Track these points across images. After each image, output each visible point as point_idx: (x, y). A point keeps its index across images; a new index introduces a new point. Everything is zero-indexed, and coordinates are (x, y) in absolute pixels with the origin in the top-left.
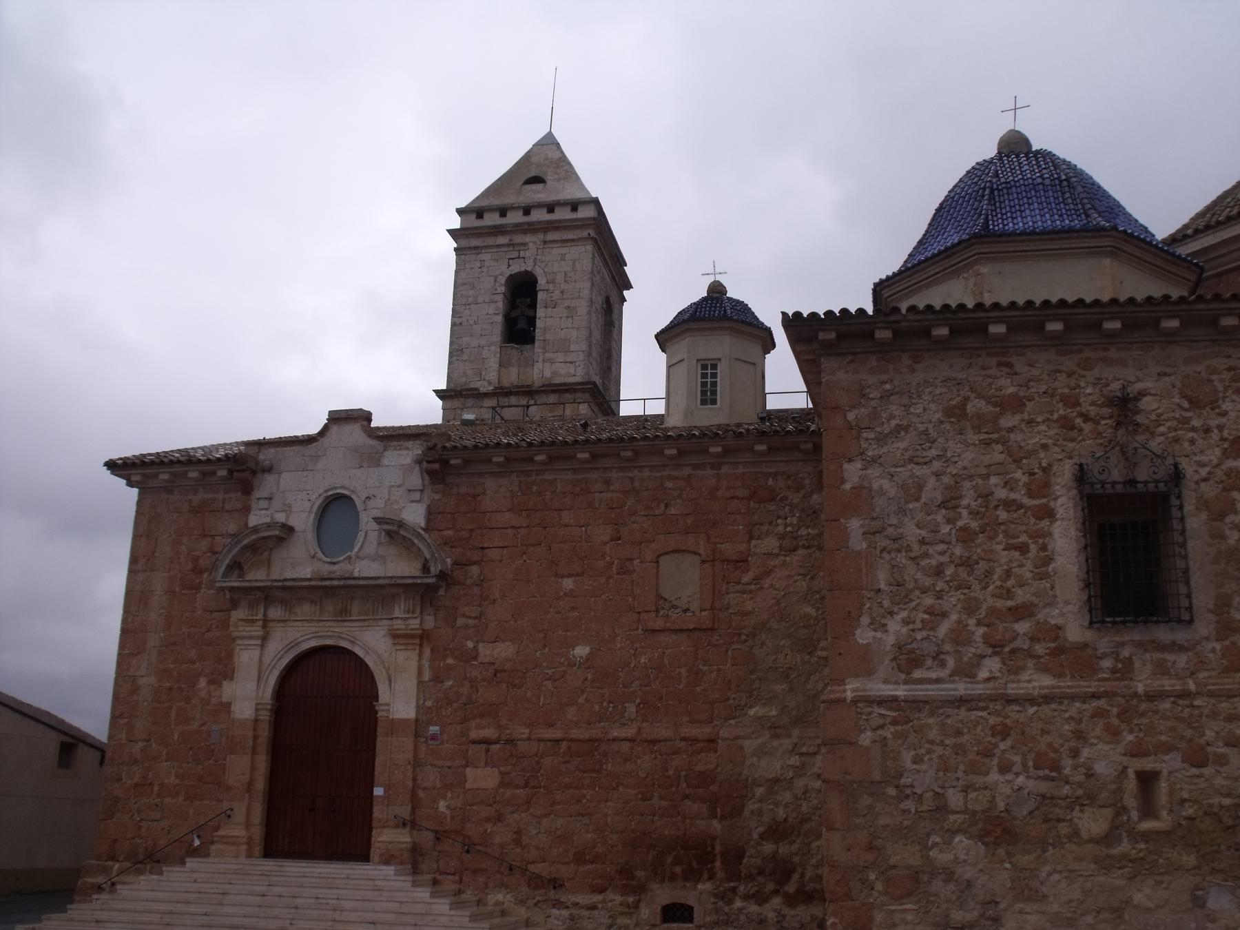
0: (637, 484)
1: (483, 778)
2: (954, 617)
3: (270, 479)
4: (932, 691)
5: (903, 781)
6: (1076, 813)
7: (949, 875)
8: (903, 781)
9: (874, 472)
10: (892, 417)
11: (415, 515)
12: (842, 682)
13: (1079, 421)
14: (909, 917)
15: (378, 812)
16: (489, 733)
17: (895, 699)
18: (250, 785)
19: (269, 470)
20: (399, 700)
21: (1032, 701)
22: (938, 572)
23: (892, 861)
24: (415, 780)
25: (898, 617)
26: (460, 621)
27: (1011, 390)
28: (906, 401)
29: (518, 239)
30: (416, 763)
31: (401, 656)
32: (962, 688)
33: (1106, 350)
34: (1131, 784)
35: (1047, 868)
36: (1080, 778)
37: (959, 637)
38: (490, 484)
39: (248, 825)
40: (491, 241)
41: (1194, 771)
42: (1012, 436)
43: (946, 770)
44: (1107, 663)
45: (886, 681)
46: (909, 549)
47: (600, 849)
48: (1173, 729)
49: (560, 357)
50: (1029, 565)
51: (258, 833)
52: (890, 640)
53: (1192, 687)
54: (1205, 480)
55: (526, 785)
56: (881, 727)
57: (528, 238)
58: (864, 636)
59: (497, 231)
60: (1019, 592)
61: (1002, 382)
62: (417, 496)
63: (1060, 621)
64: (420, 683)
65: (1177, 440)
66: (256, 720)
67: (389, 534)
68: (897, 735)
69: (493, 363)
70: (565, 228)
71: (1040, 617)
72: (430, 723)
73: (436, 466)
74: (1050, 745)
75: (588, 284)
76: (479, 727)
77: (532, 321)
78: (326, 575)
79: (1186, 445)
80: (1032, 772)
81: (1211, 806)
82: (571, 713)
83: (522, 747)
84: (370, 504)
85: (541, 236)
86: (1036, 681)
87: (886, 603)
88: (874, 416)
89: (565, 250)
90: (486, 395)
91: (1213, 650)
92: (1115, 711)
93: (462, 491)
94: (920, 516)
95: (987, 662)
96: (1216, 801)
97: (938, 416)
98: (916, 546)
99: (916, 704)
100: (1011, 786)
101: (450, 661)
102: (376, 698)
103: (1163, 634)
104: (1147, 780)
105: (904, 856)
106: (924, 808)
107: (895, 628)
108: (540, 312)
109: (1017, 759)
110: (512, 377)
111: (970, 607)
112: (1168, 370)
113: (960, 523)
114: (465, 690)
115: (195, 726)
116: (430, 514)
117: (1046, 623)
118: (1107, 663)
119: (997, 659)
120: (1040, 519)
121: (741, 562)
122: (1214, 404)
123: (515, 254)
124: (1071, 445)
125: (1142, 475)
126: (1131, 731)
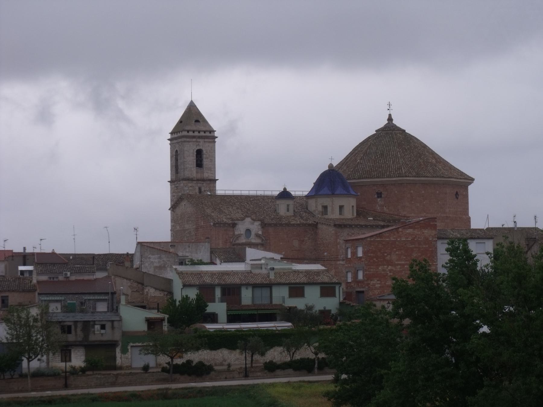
11: (260, 233)
29: (198, 140)
40: (191, 140)
49: (209, 172)
57: (200, 140)
59: (194, 137)
69: (195, 172)
85: (203, 140)
110: (199, 176)
116: (262, 233)
121: (303, 241)
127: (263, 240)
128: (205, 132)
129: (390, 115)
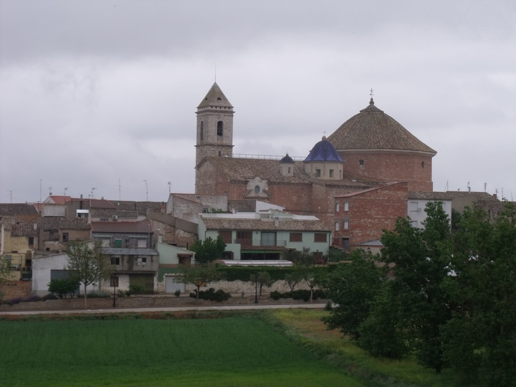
11: (267, 189)
29: (220, 114)
40: (214, 113)
57: (221, 114)
59: (216, 111)
110: (219, 142)
121: (300, 197)
127: (268, 195)
128: (225, 108)
129: (372, 99)
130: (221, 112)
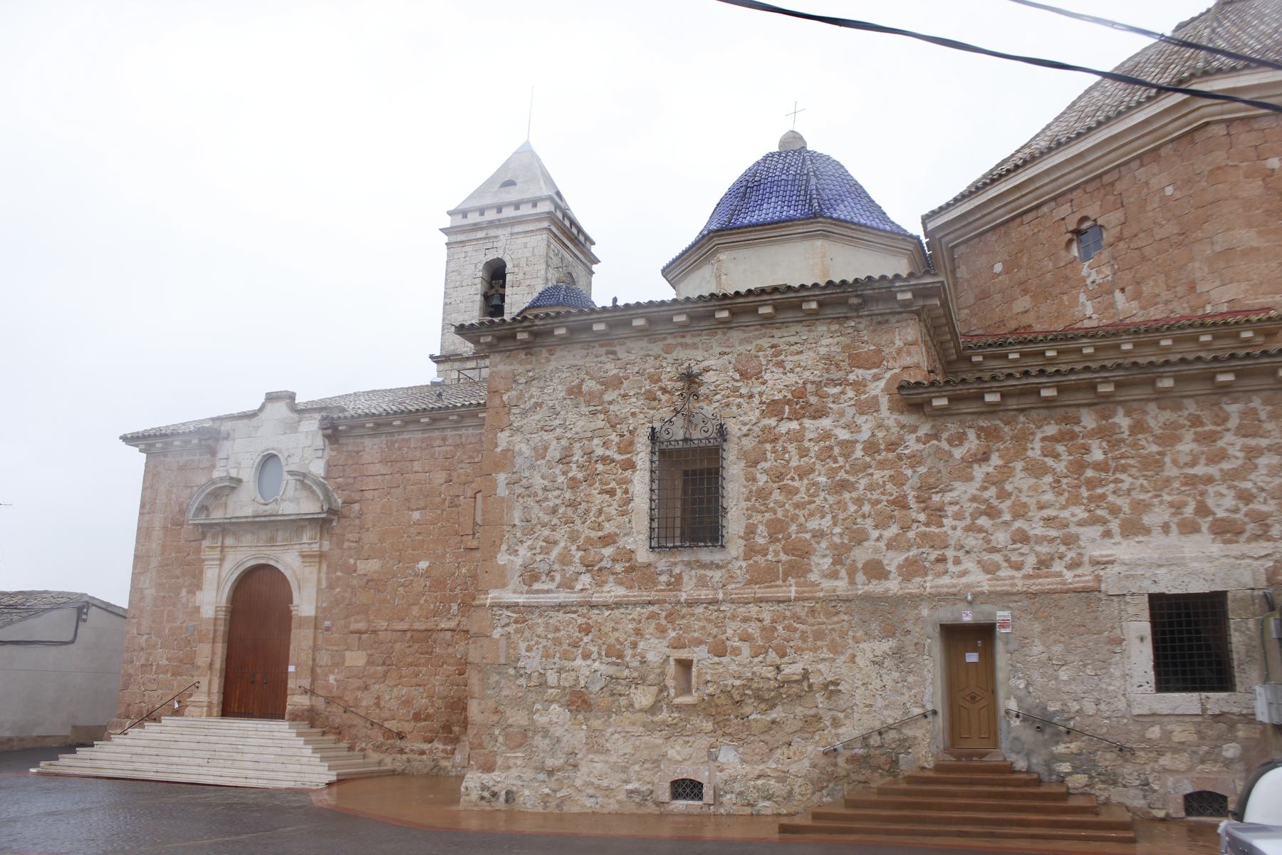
0: (463, 440)
1: (356, 659)
2: (562, 544)
3: (227, 444)
4: (542, 599)
5: (520, 664)
6: (632, 690)
7: (546, 733)
8: (520, 664)
9: (517, 438)
10: (532, 396)
11: (317, 468)
12: (487, 593)
13: (659, 393)
14: (519, 762)
15: (291, 684)
16: (362, 626)
17: (517, 605)
18: (211, 664)
19: (227, 437)
20: (305, 604)
21: (607, 606)
22: (554, 511)
23: (510, 722)
24: (314, 660)
25: (525, 545)
26: (346, 545)
27: (615, 371)
28: (542, 384)
29: (492, 233)
30: (315, 648)
31: (307, 570)
32: (562, 597)
33: (683, 337)
34: (672, 668)
35: (611, 730)
36: (636, 664)
37: (565, 560)
38: (368, 442)
39: (209, 693)
40: (472, 236)
41: (716, 659)
42: (612, 407)
43: (547, 657)
44: (664, 578)
45: (515, 592)
46: (536, 495)
47: (431, 711)
48: (704, 628)
50: (615, 505)
51: (216, 698)
52: (519, 561)
53: (720, 596)
54: (746, 435)
55: (384, 663)
56: (507, 625)
57: (500, 232)
58: (502, 558)
59: (476, 227)
60: (607, 525)
61: (610, 366)
62: (320, 453)
63: (633, 547)
64: (319, 591)
65: (728, 405)
66: (216, 619)
67: (302, 482)
68: (517, 631)
70: (526, 222)
71: (621, 544)
72: (325, 619)
73: (329, 432)
74: (617, 640)
75: (544, 266)
76: (356, 621)
77: (502, 297)
78: (261, 512)
79: (735, 408)
80: (605, 659)
81: (726, 686)
82: (415, 611)
83: (382, 635)
84: (290, 460)
85: (509, 230)
86: (613, 591)
87: (519, 535)
88: (520, 397)
89: (527, 240)
90: (468, 359)
91: (740, 568)
92: (664, 614)
93: (350, 448)
94: (544, 470)
95: (582, 577)
96: (730, 682)
97: (563, 394)
98: (540, 492)
99: (530, 608)
100: (589, 670)
101: (339, 574)
102: (291, 601)
103: (705, 555)
104: (685, 665)
105: (517, 718)
106: (532, 684)
107: (523, 551)
108: (508, 291)
109: (595, 649)
111: (573, 537)
112: (727, 350)
113: (570, 475)
114: (348, 595)
115: (178, 624)
116: (329, 466)
117: (624, 548)
118: (664, 578)
119: (588, 575)
120: (625, 470)
122: (758, 376)
123: (490, 245)
124: (652, 412)
125: (696, 435)
126: (674, 629)
130: (492, 224)
